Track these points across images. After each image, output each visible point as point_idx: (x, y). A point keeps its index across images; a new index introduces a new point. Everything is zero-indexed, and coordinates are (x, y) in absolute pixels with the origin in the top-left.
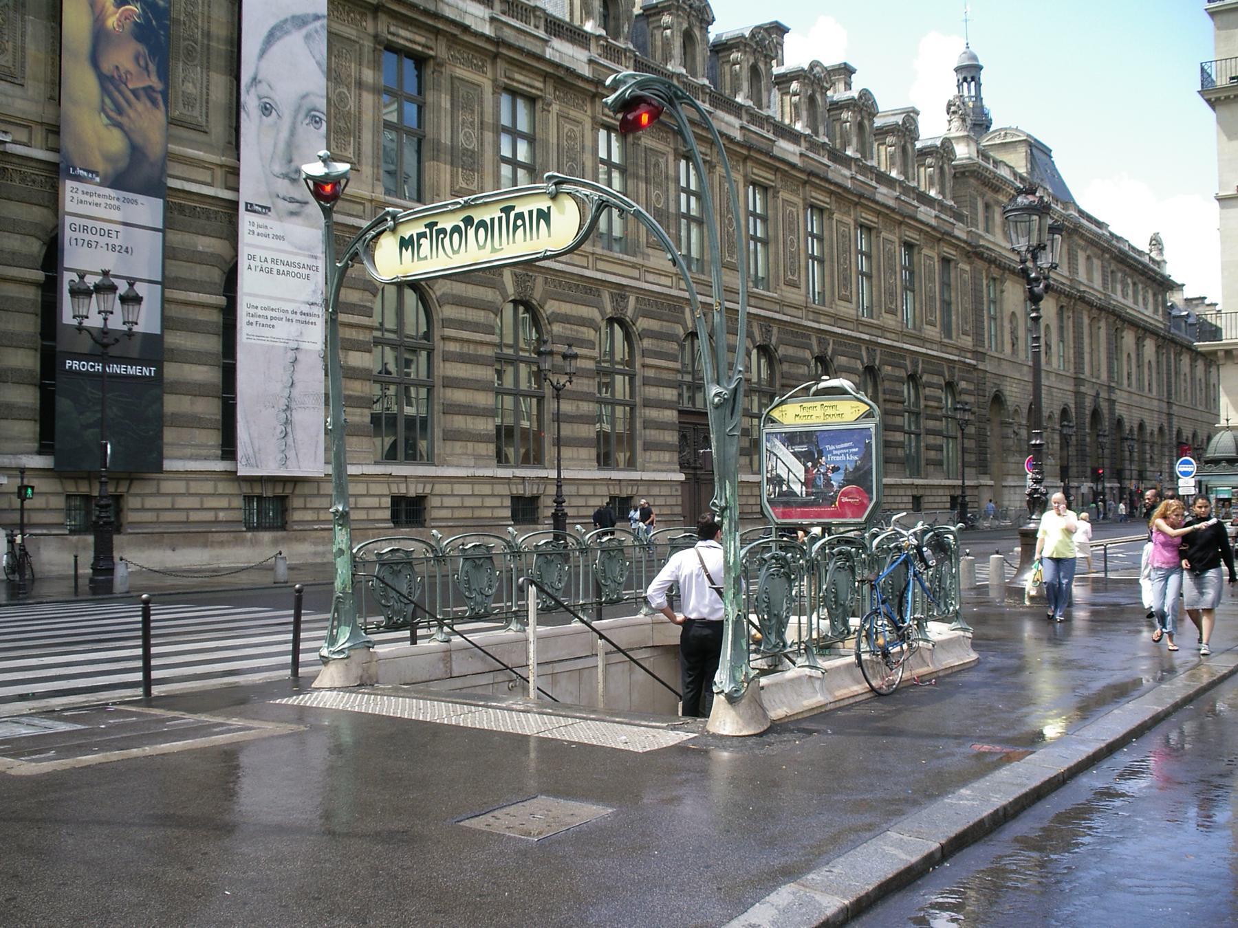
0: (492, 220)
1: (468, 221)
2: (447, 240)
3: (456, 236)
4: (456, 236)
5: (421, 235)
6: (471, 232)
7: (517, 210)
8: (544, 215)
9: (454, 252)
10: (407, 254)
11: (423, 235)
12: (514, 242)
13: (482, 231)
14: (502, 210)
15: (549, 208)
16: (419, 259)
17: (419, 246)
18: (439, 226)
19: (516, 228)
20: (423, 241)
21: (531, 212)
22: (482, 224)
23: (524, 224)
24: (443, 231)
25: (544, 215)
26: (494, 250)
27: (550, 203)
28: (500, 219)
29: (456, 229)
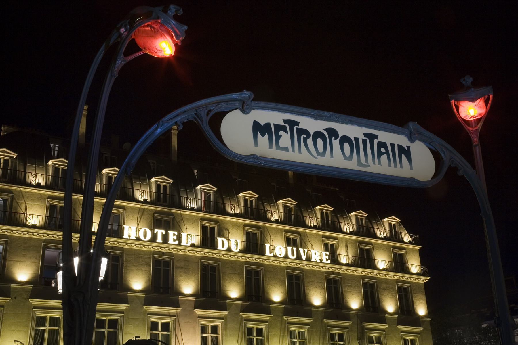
0: (357, 140)
1: (333, 133)
2: (310, 141)
3: (320, 141)
4: (320, 141)
5: (278, 128)
6: (336, 143)
7: (380, 139)
8: (405, 152)
9: (318, 153)
10: (263, 140)
11: (284, 129)
12: (380, 163)
13: (346, 146)
14: (366, 135)
15: (409, 148)
16: (278, 147)
17: (278, 137)
18: (300, 126)
19: (380, 154)
20: (281, 133)
21: (393, 145)
22: (345, 139)
23: (387, 152)
24: (306, 132)
25: (405, 152)
26: (360, 164)
27: (409, 144)
28: (364, 141)
29: (318, 135)
